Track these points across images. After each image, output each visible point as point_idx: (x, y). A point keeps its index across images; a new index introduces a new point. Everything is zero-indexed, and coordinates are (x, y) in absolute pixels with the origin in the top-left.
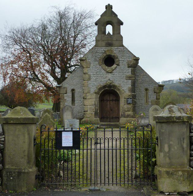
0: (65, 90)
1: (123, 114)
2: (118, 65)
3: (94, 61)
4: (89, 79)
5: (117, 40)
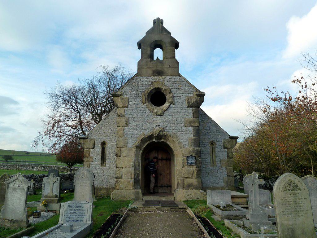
0: (92, 142)
1: (180, 183)
2: (172, 103)
4: (127, 123)
5: (170, 67)
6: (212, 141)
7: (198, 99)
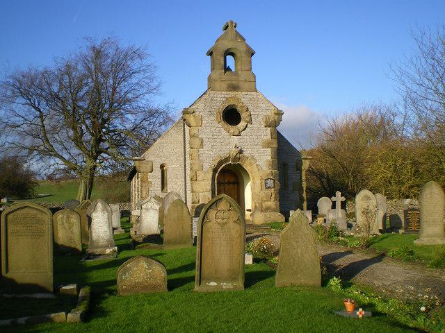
0: (150, 165)
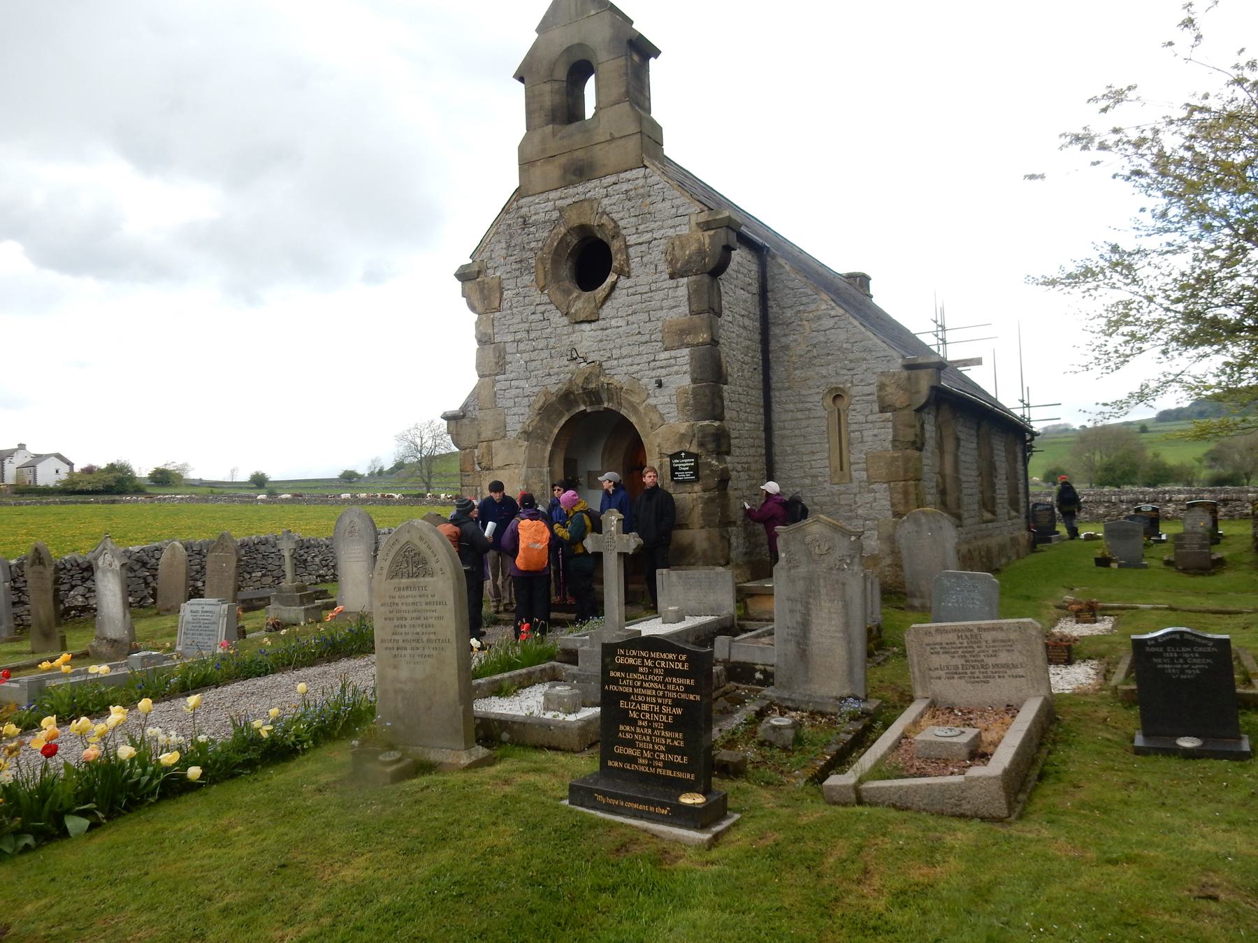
3: (518, 273)
5: (613, 139)
6: (834, 386)
7: (707, 241)
